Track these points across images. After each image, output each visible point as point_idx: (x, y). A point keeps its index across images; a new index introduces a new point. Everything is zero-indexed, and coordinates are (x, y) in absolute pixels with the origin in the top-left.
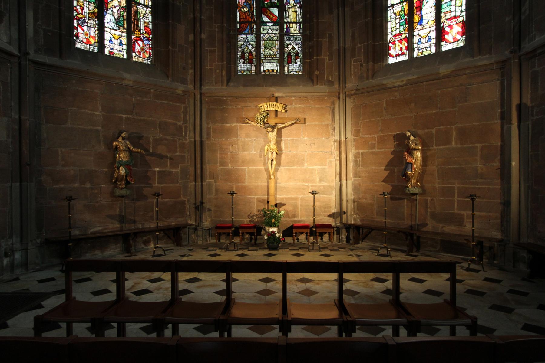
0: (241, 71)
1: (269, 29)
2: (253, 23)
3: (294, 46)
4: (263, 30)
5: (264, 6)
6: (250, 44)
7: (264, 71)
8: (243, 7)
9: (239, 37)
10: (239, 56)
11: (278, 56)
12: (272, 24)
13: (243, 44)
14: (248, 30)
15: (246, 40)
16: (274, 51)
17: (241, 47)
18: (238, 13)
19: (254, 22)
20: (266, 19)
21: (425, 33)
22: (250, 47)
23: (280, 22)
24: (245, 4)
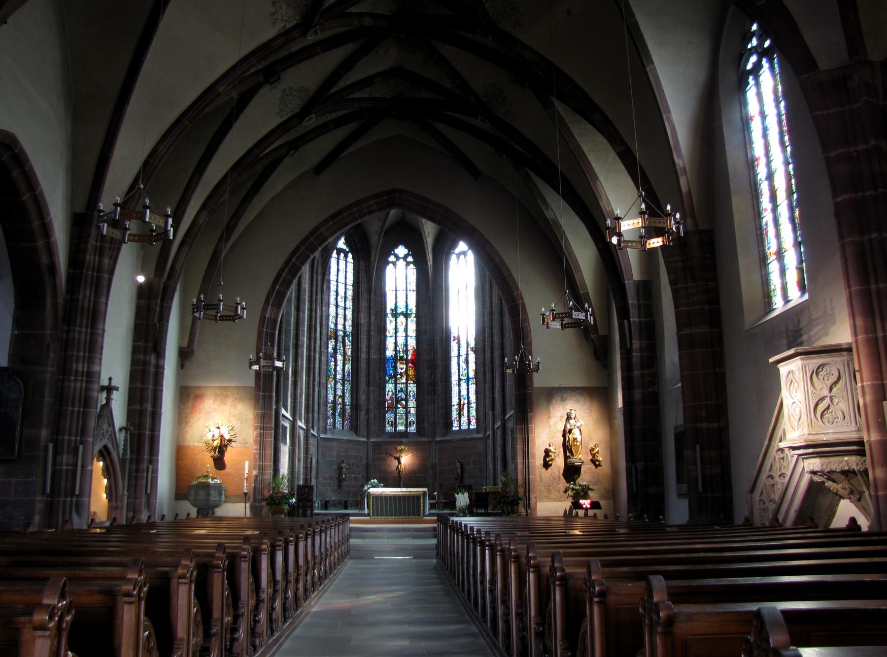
1: (401, 411)
3: (412, 418)
15: (390, 416)
21: (464, 419)
23: (406, 407)
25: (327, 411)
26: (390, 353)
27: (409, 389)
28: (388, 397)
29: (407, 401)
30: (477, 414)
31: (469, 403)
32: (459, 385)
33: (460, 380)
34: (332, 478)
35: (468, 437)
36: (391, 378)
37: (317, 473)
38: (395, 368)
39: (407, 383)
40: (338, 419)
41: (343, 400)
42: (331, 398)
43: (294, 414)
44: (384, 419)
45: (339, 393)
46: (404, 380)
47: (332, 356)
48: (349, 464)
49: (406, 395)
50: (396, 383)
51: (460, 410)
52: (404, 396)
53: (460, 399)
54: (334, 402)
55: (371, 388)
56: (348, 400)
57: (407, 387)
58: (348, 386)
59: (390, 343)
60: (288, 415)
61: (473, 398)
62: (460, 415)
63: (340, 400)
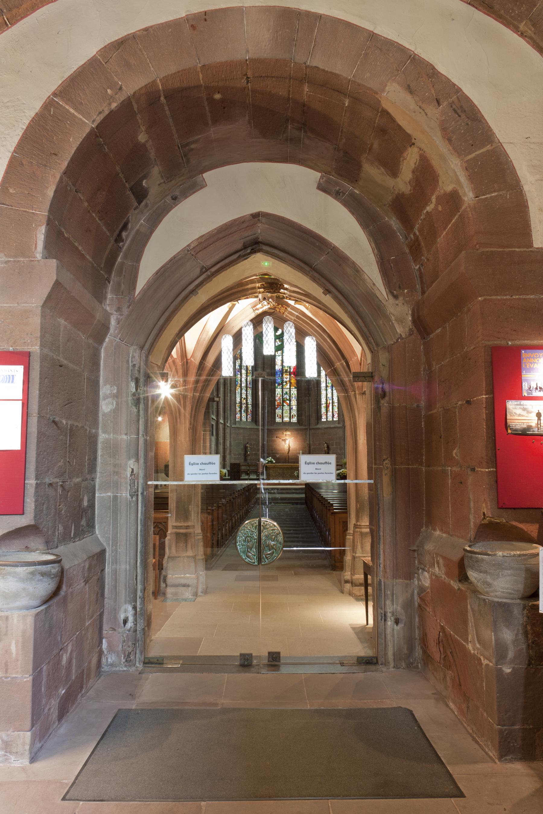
1: (286, 408)
3: (294, 412)
15: (278, 411)
16: (288, 414)
20: (285, 404)
21: (330, 414)
23: (290, 405)
25: (236, 408)
26: (278, 367)
27: (292, 392)
28: (277, 398)
29: (290, 400)
30: (338, 411)
31: (333, 403)
32: (326, 390)
33: (327, 386)
34: (240, 454)
35: (332, 426)
36: (279, 385)
37: (230, 451)
39: (290, 388)
40: (244, 414)
41: (247, 401)
42: (238, 400)
43: (217, 416)
45: (244, 396)
46: (288, 386)
47: (238, 371)
48: (251, 444)
49: (290, 397)
50: (282, 389)
51: (327, 407)
52: (288, 398)
53: (327, 400)
54: (241, 403)
55: (266, 392)
56: (250, 401)
57: (290, 391)
58: (250, 391)
60: (214, 418)
61: (336, 400)
62: (327, 411)
63: (244, 401)
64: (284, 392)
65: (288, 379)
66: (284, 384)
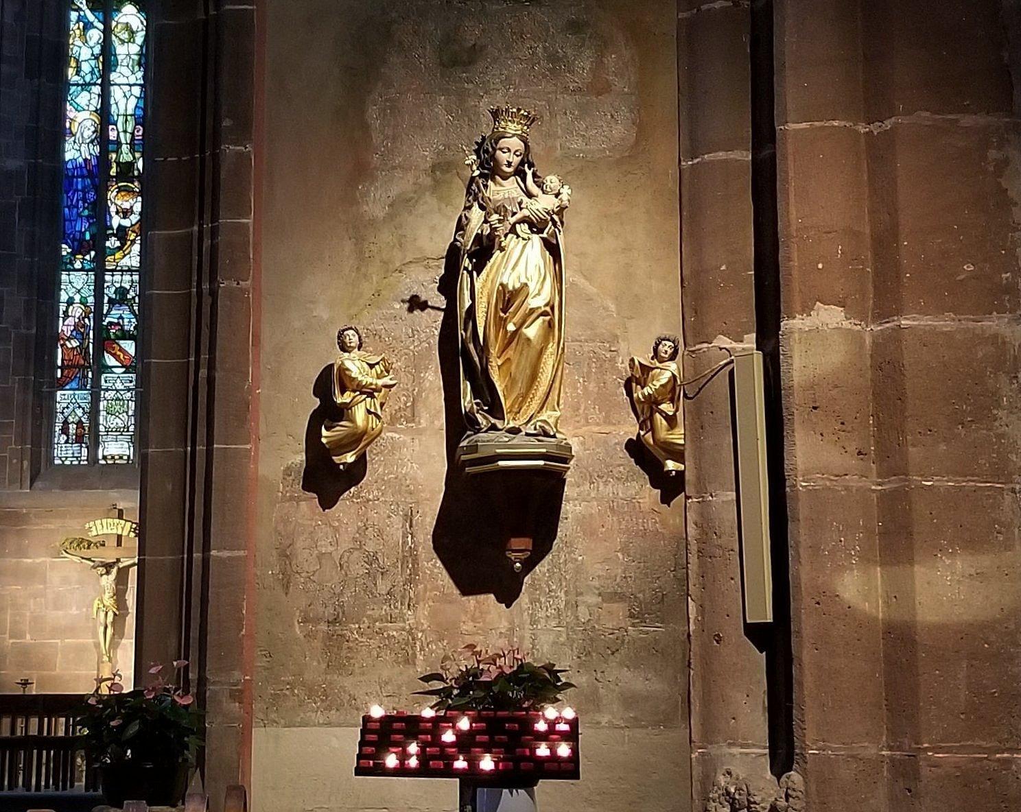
0: (60, 458)
2: (87, 367)
4: (106, 381)
5: (109, 338)
6: (80, 407)
7: (105, 458)
8: (69, 339)
9: (59, 393)
10: (57, 429)
11: (132, 428)
12: (123, 370)
13: (67, 407)
14: (77, 379)
17: (63, 413)
18: (60, 350)
19: (90, 367)
20: (110, 361)
22: (79, 412)
24: (74, 333)
26: (77, 150)
28: (65, 327)
36: (80, 247)
38: (99, 211)
44: (44, 410)
50: (99, 270)
59: (81, 114)
64: (110, 292)
65: (135, 218)
66: (113, 243)
